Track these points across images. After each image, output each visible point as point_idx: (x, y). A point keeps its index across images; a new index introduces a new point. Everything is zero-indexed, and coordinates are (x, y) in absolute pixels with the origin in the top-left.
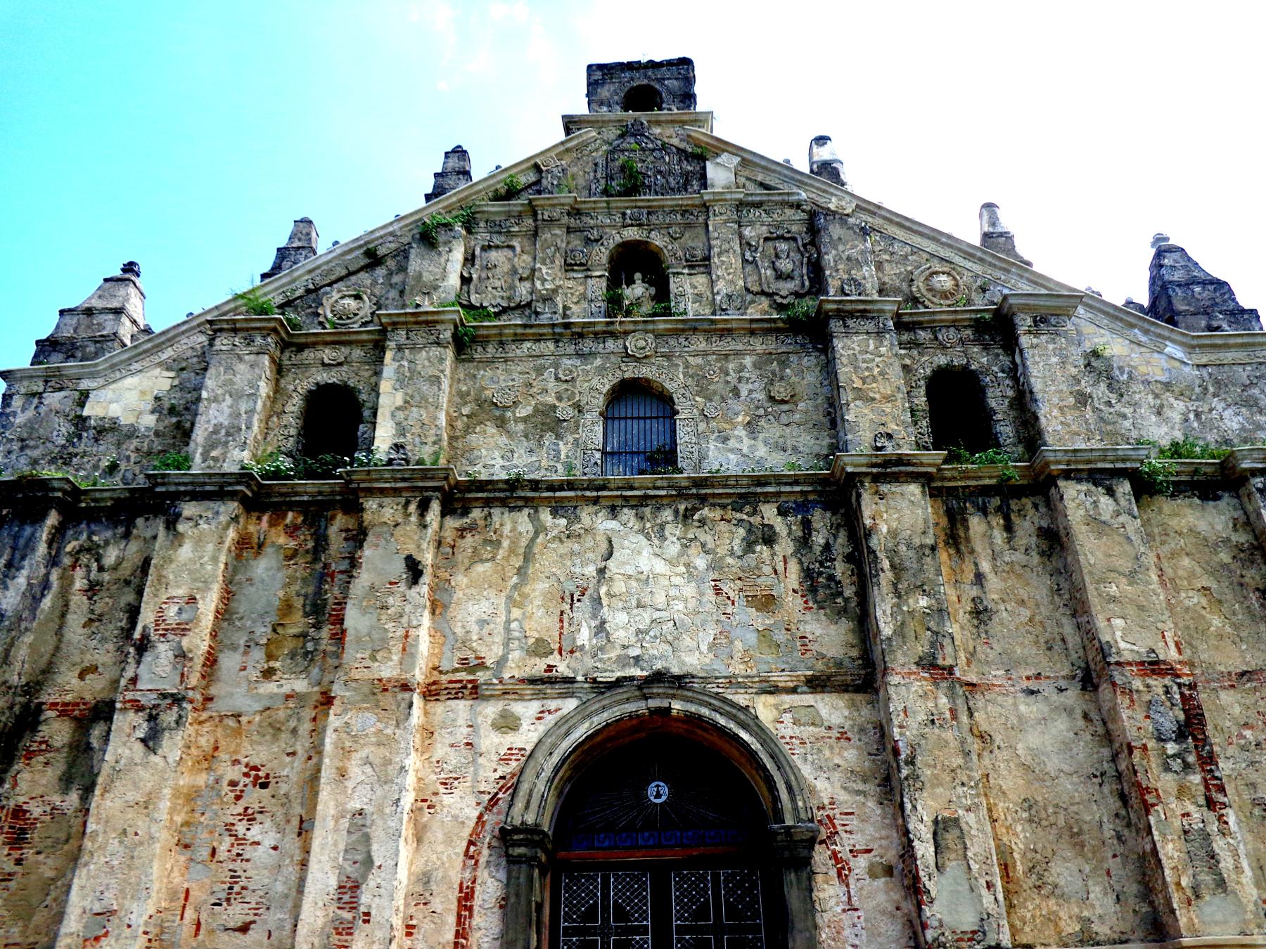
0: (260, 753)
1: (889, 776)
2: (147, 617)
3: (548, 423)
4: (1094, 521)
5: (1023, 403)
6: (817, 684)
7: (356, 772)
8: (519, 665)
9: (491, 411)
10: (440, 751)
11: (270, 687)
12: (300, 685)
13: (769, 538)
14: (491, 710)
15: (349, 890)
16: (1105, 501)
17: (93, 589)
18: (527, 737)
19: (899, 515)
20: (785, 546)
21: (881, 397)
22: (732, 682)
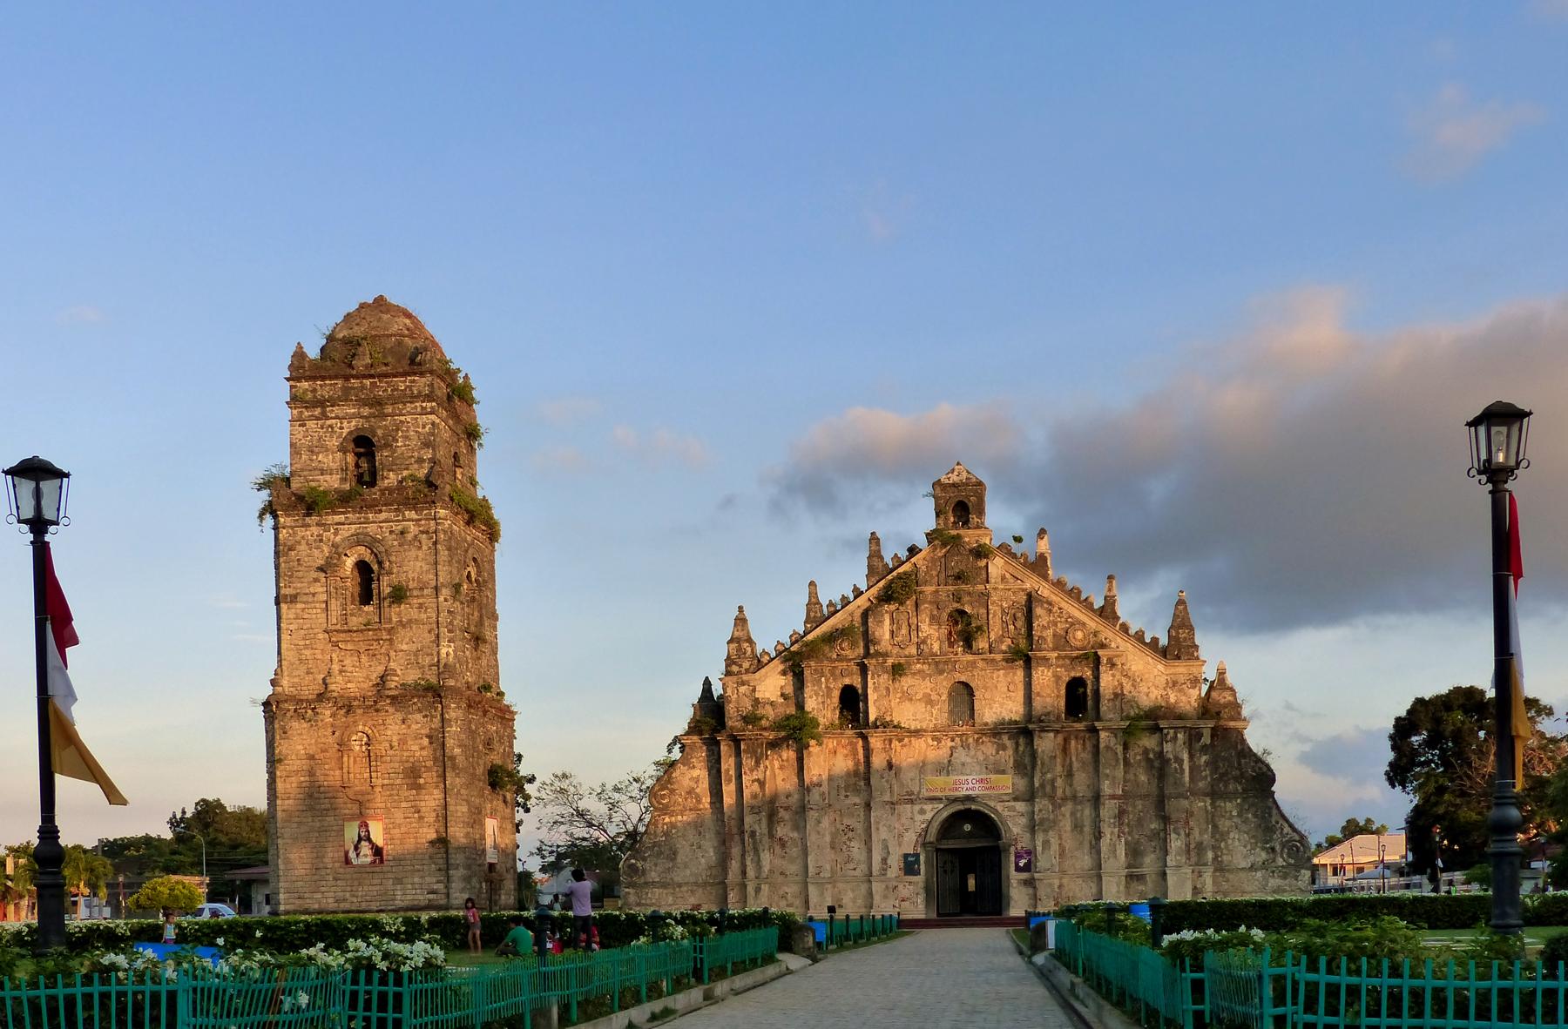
0: (847, 821)
1: (1032, 828)
2: (807, 781)
3: (929, 702)
4: (1107, 747)
5: (1097, 692)
6: (1016, 799)
7: (883, 829)
8: (925, 793)
9: (907, 697)
10: (903, 820)
11: (848, 801)
12: (857, 800)
13: (1004, 748)
14: (917, 808)
15: (884, 861)
16: (1113, 740)
17: (781, 768)
18: (929, 816)
19: (1046, 744)
20: (1010, 752)
21: (1049, 685)
22: (990, 797)
